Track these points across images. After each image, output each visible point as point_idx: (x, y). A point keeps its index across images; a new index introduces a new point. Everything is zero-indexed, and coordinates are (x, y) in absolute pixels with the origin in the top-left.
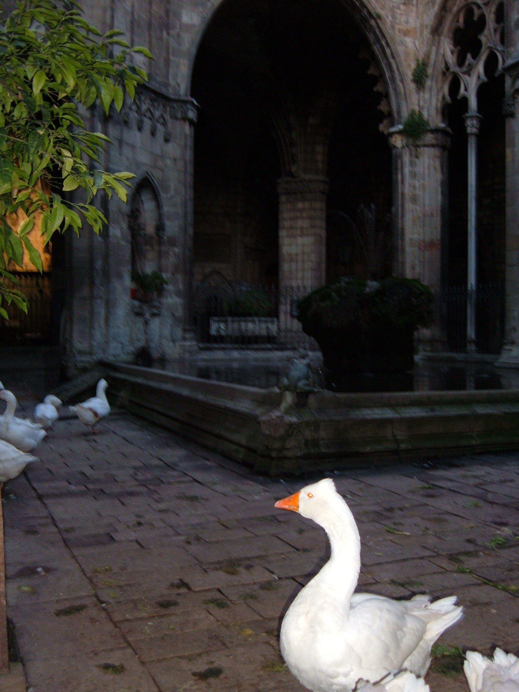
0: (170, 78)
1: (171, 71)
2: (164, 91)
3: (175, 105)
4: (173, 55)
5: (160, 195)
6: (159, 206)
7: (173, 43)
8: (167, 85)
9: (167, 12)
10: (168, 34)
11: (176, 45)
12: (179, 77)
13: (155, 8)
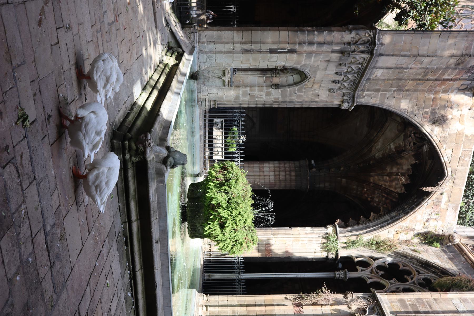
2: (360, 88)
4: (381, 94)
6: (290, 85)
7: (388, 94)
9: (407, 90)
10: (395, 91)
11: (387, 96)
12: (368, 98)
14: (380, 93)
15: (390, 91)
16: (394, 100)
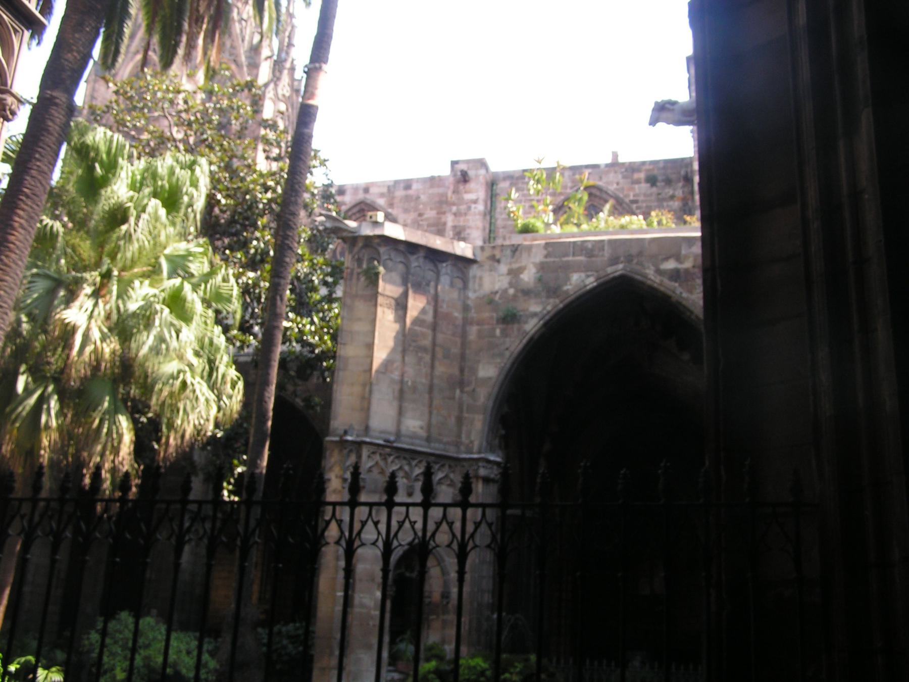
0: (463, 436)
1: (464, 428)
3: (465, 464)
5: (444, 561)
8: (457, 444)
9: (462, 370)
10: (462, 391)
13: (440, 369)
14: (466, 415)
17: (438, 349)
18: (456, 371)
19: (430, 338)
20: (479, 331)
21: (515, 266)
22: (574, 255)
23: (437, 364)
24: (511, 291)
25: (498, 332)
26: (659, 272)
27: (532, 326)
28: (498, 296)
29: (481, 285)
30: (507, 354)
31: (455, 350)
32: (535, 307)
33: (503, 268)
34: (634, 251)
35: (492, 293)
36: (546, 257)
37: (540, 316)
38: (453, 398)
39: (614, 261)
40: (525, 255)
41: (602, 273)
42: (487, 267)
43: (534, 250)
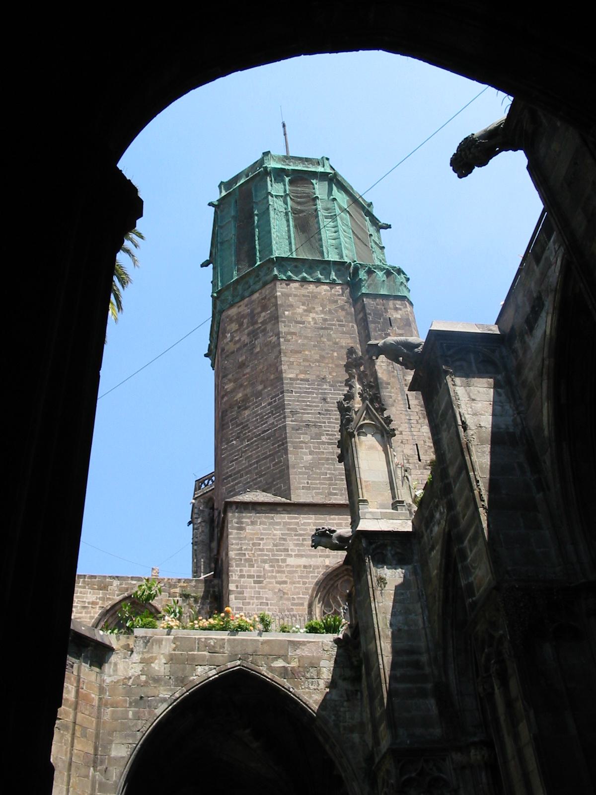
10: (95, 770)
13: (78, 746)
15: (94, 777)
16: (111, 768)
17: (77, 727)
18: (92, 751)
19: (71, 717)
20: (113, 712)
21: (147, 656)
22: (198, 651)
23: (75, 741)
24: (143, 678)
25: (130, 714)
26: (271, 669)
27: (161, 710)
28: (131, 681)
29: (115, 671)
30: (139, 735)
31: (91, 730)
32: (164, 694)
33: (136, 657)
34: (250, 650)
35: (126, 678)
36: (174, 650)
37: (169, 702)
38: (87, 776)
39: (233, 658)
40: (156, 648)
41: (223, 668)
42: (121, 655)
43: (164, 643)
